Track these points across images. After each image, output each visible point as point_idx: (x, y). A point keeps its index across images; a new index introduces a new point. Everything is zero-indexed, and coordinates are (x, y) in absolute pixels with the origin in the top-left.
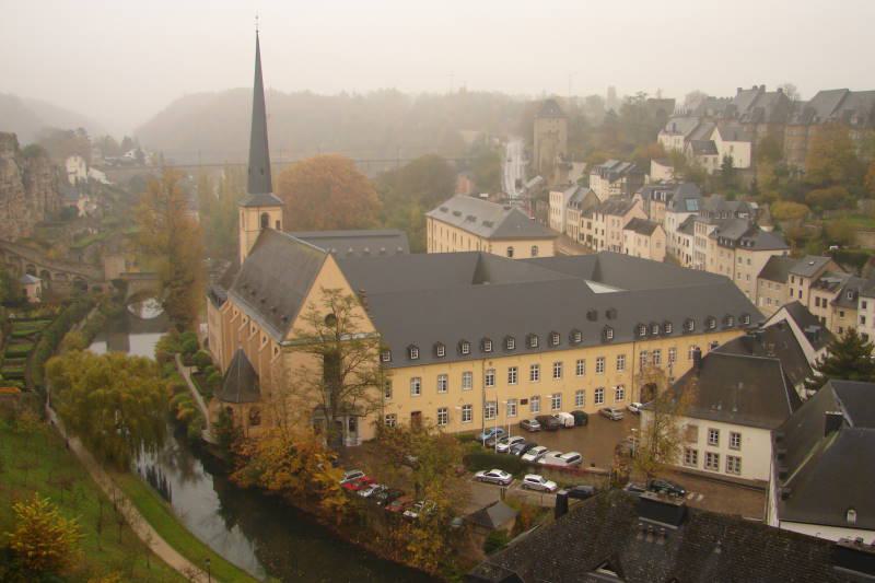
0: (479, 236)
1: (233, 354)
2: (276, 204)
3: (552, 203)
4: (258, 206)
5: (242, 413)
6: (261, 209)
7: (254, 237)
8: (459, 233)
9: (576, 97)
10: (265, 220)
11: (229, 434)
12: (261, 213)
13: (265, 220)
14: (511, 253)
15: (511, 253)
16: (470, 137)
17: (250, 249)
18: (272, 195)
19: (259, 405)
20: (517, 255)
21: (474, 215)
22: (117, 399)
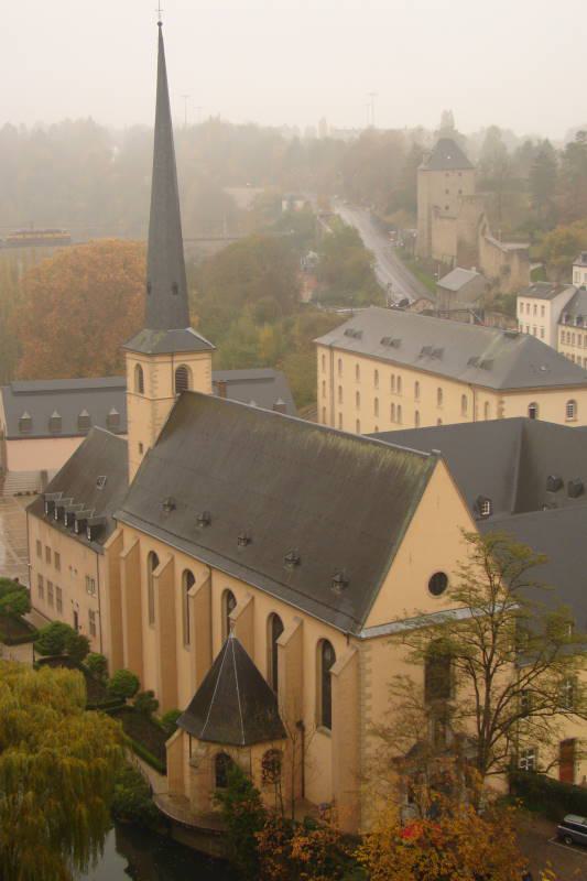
0: (470, 385)
1: (218, 648)
2: (195, 348)
3: (519, 316)
4: (172, 354)
5: (252, 759)
6: (176, 358)
7: (165, 409)
8: (448, 387)
9: (420, 130)
10: (181, 377)
11: (254, 816)
12: (176, 366)
13: (181, 377)
14: (533, 412)
15: (533, 412)
16: (243, 196)
17: (158, 434)
18: (190, 329)
19: (281, 745)
20: (543, 416)
21: (395, 336)
22: (52, 769)
